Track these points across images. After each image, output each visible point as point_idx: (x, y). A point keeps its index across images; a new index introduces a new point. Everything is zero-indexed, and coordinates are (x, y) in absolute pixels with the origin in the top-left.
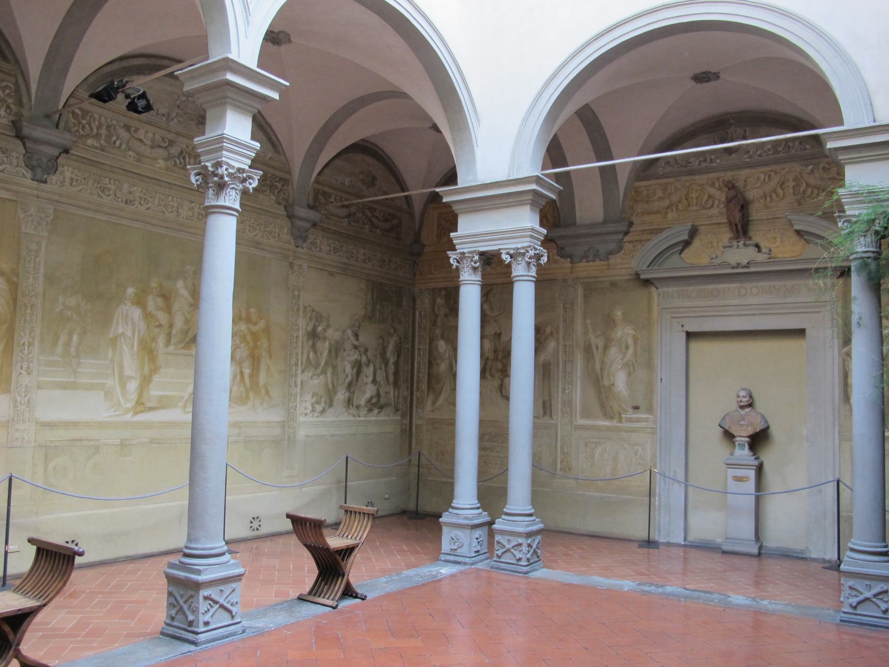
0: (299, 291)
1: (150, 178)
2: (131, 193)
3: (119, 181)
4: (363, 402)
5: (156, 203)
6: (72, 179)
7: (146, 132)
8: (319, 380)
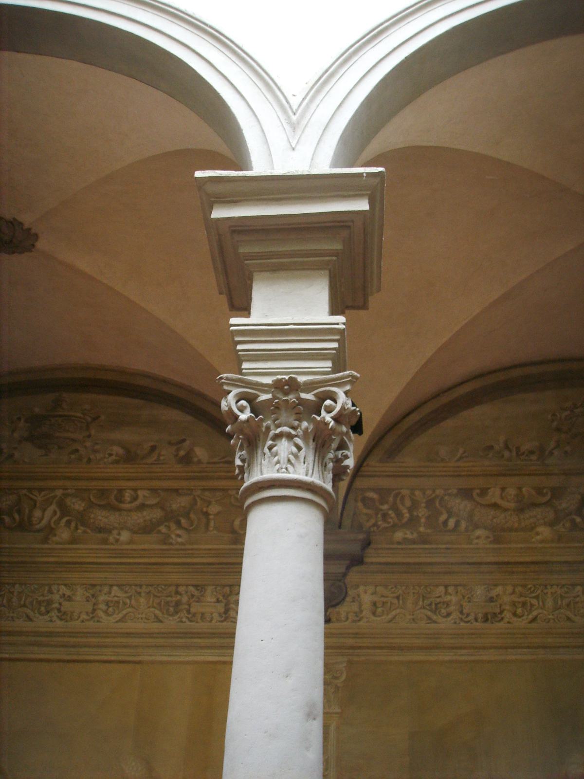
1: (527, 563)
2: (491, 600)
3: (464, 586)
5: (550, 603)
6: (375, 604)
7: (503, 489)
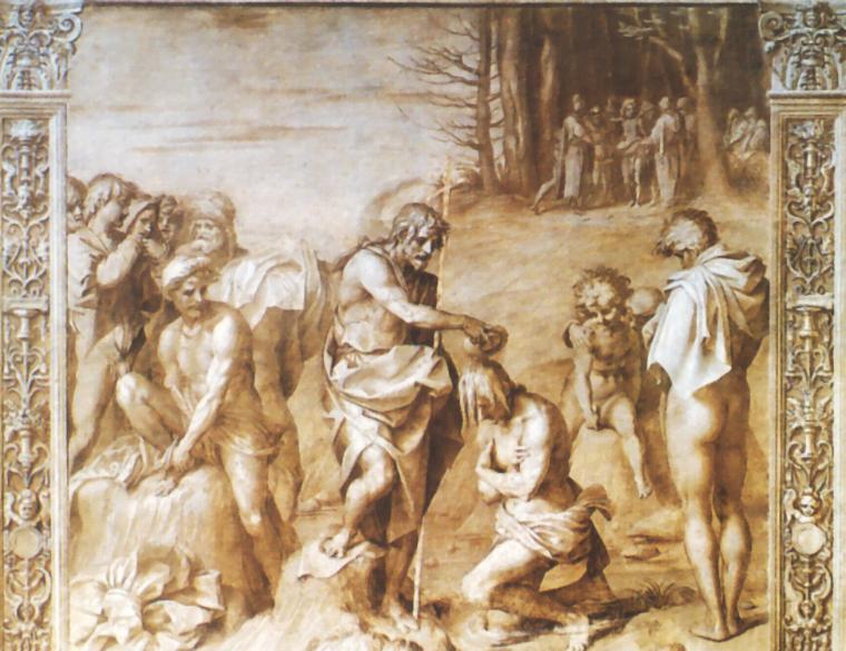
0: (39, 119)
4: (476, 584)
8: (177, 494)
